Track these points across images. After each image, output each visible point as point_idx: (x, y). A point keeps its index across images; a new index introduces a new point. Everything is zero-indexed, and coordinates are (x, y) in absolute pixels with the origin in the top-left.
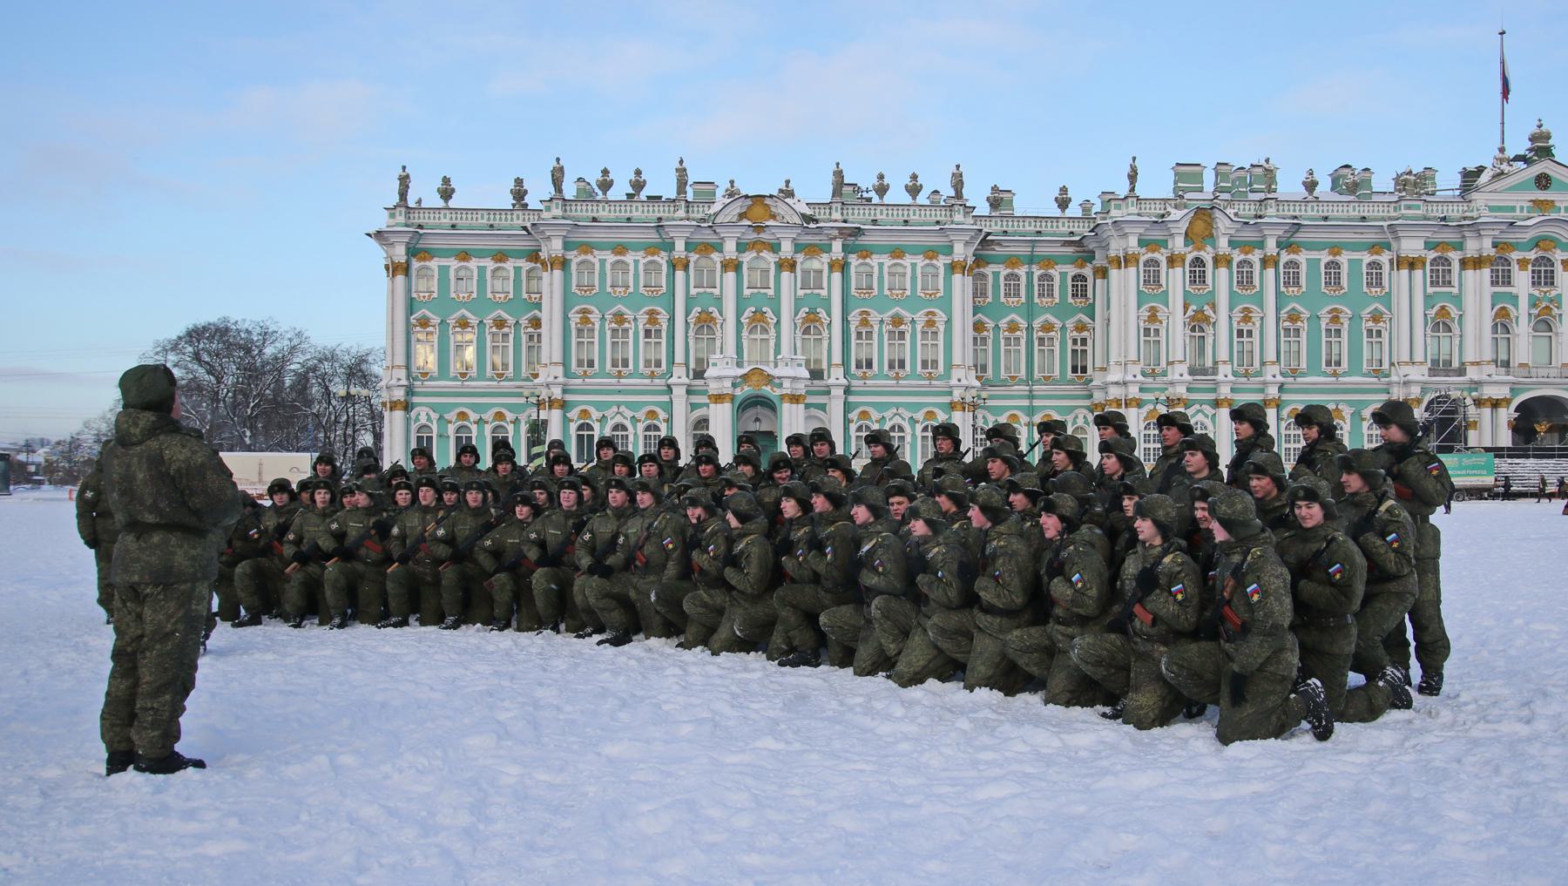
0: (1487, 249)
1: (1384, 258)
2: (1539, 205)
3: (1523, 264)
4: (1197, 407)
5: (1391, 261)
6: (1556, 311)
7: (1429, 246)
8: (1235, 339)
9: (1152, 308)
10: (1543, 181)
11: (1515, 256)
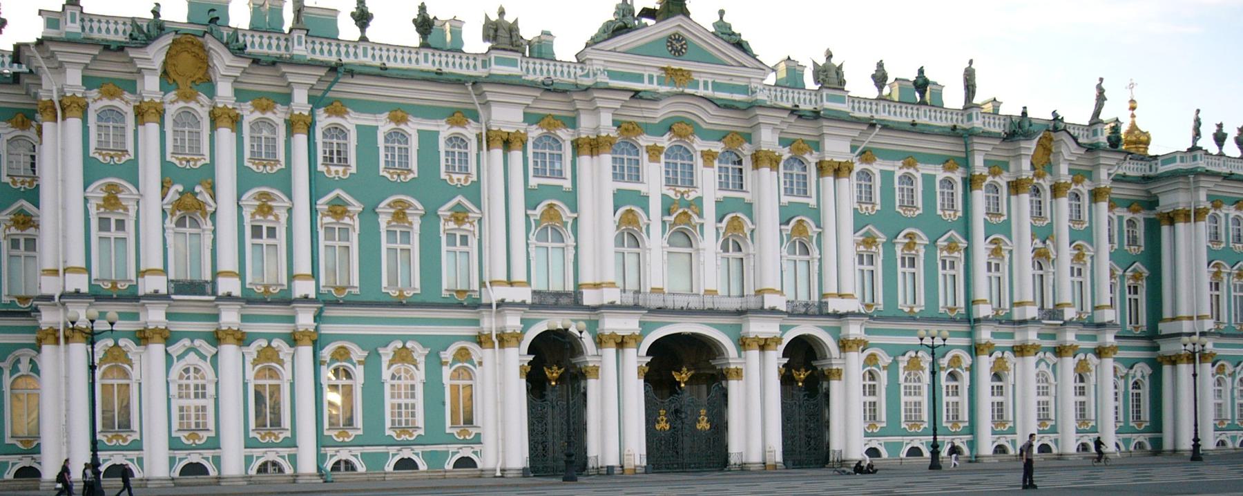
0: (606, 124)
1: (470, 131)
2: (672, 75)
3: (654, 152)
4: (186, 342)
5: (479, 137)
6: (695, 219)
7: (530, 118)
8: (249, 240)
9: (111, 185)
10: (676, 45)
11: (644, 141)
